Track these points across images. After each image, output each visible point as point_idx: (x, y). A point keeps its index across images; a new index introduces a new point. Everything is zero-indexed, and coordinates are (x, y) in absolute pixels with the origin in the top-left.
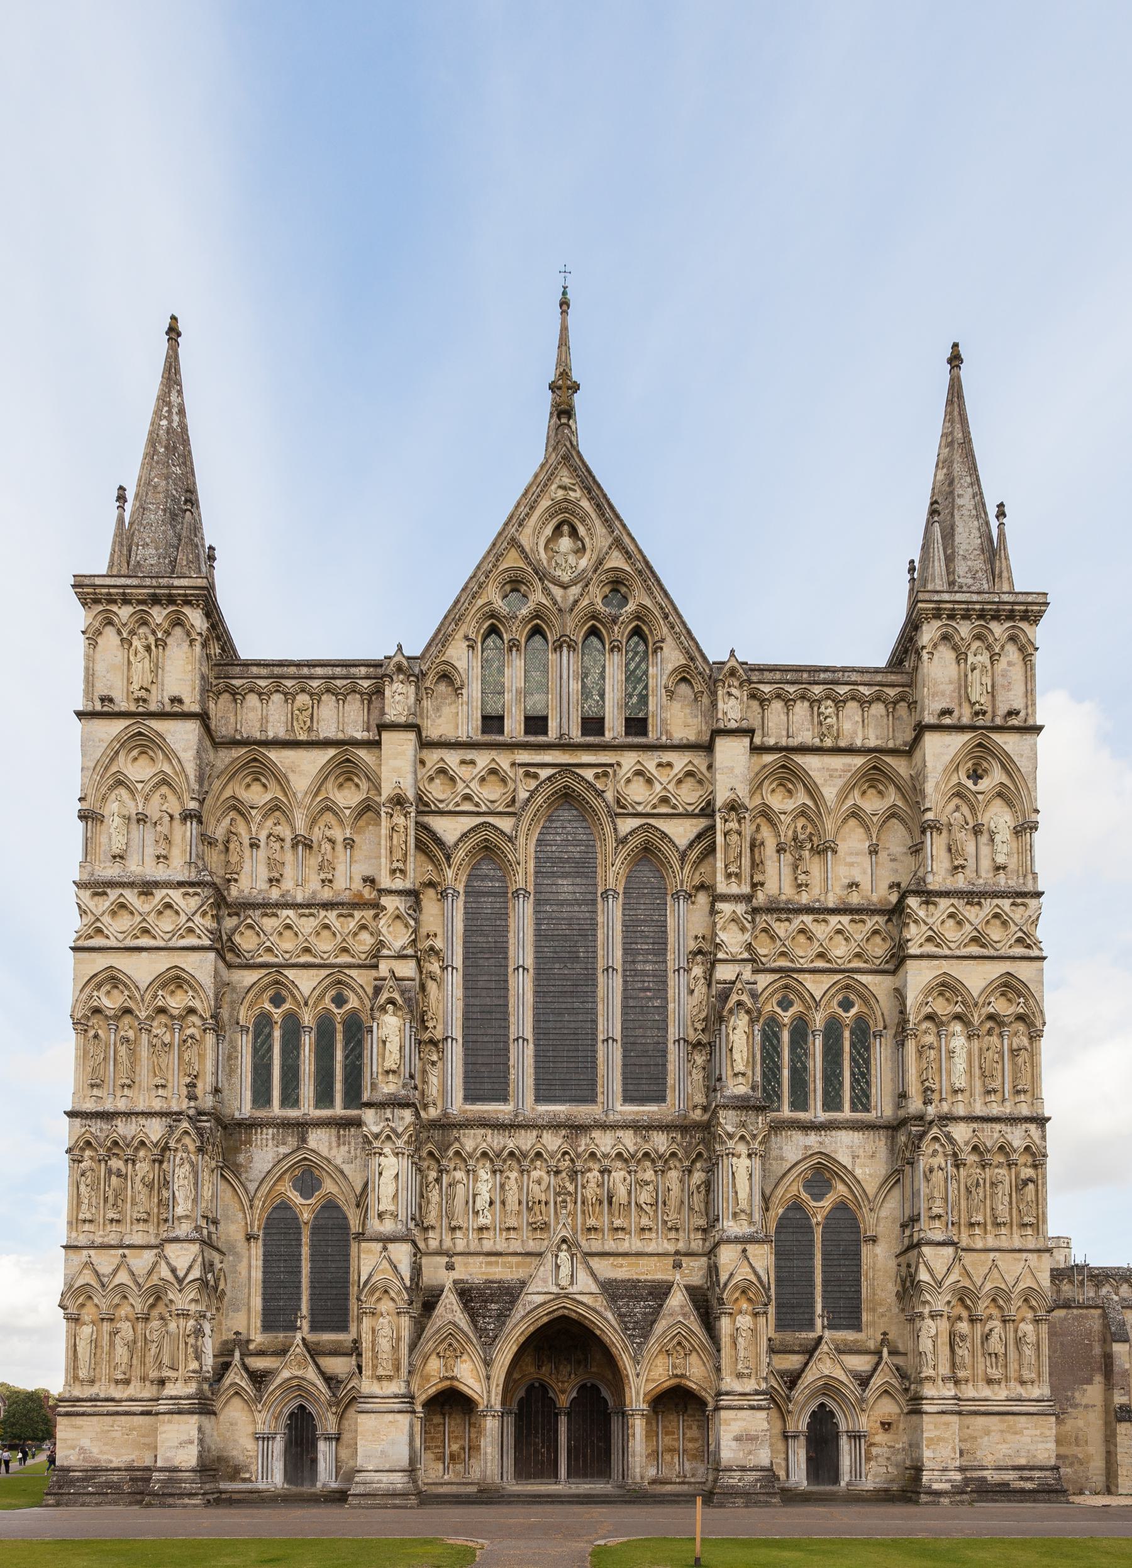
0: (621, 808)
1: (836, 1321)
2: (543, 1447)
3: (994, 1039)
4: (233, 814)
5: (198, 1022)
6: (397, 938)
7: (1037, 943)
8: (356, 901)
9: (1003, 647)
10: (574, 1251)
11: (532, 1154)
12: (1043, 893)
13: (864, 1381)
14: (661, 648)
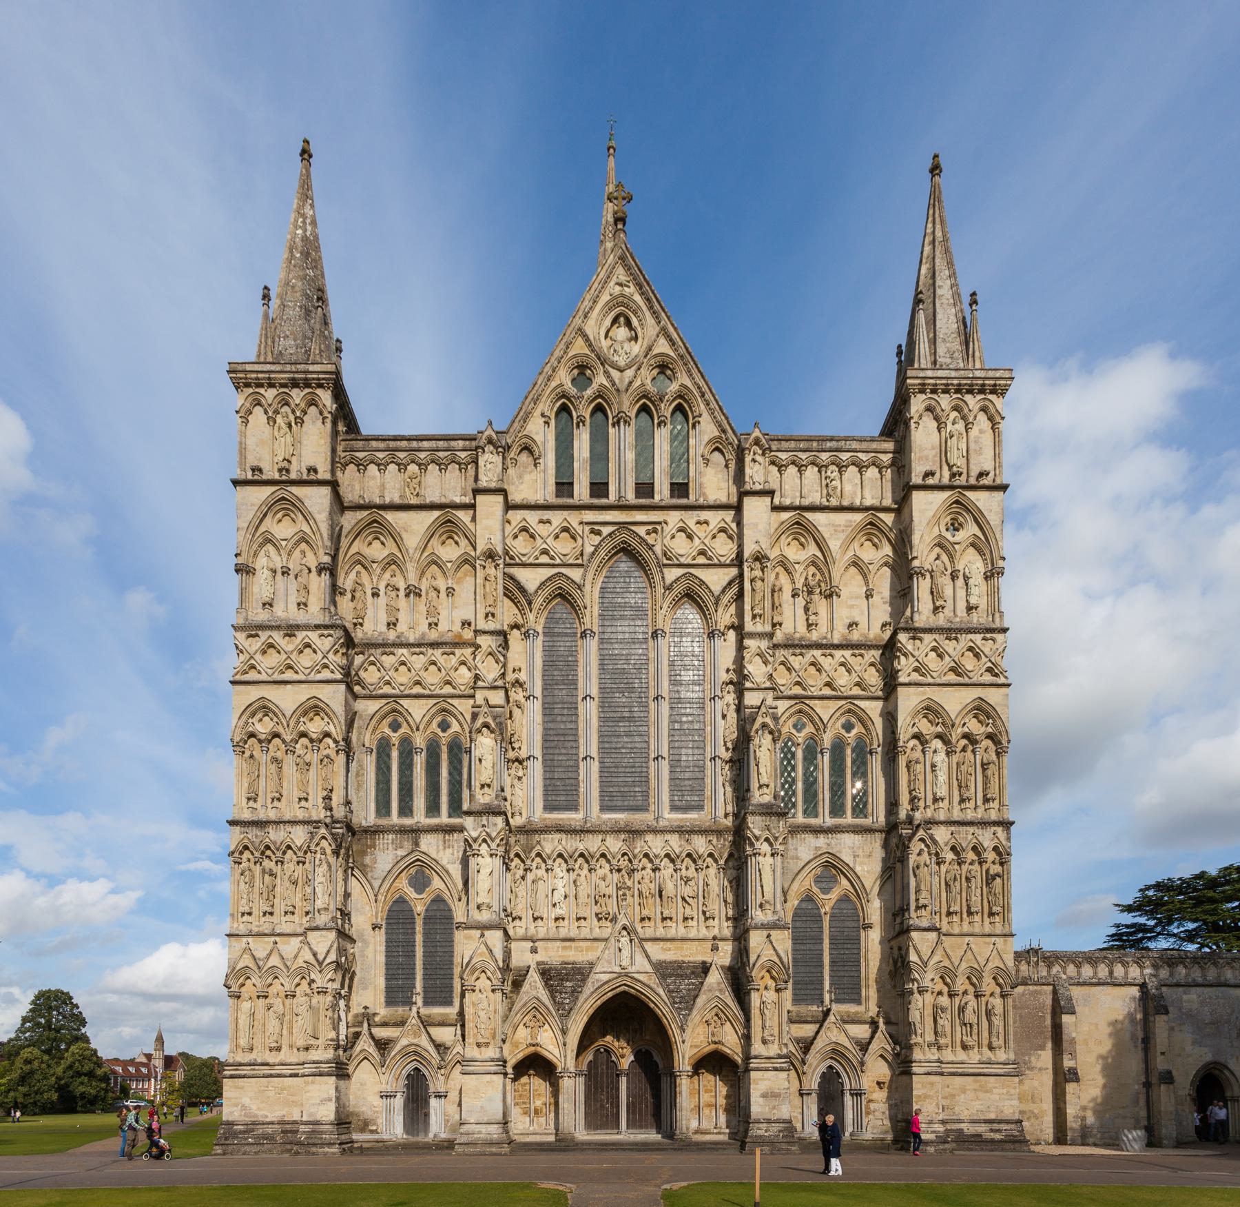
0: (670, 560)
1: (842, 996)
2: (607, 1103)
3: (969, 754)
4: (359, 567)
5: (333, 745)
6: (490, 671)
7: (1003, 672)
8: (457, 641)
9: (975, 417)
10: (633, 937)
11: (598, 855)
12: (1008, 629)
13: (864, 1047)
14: (699, 422)
